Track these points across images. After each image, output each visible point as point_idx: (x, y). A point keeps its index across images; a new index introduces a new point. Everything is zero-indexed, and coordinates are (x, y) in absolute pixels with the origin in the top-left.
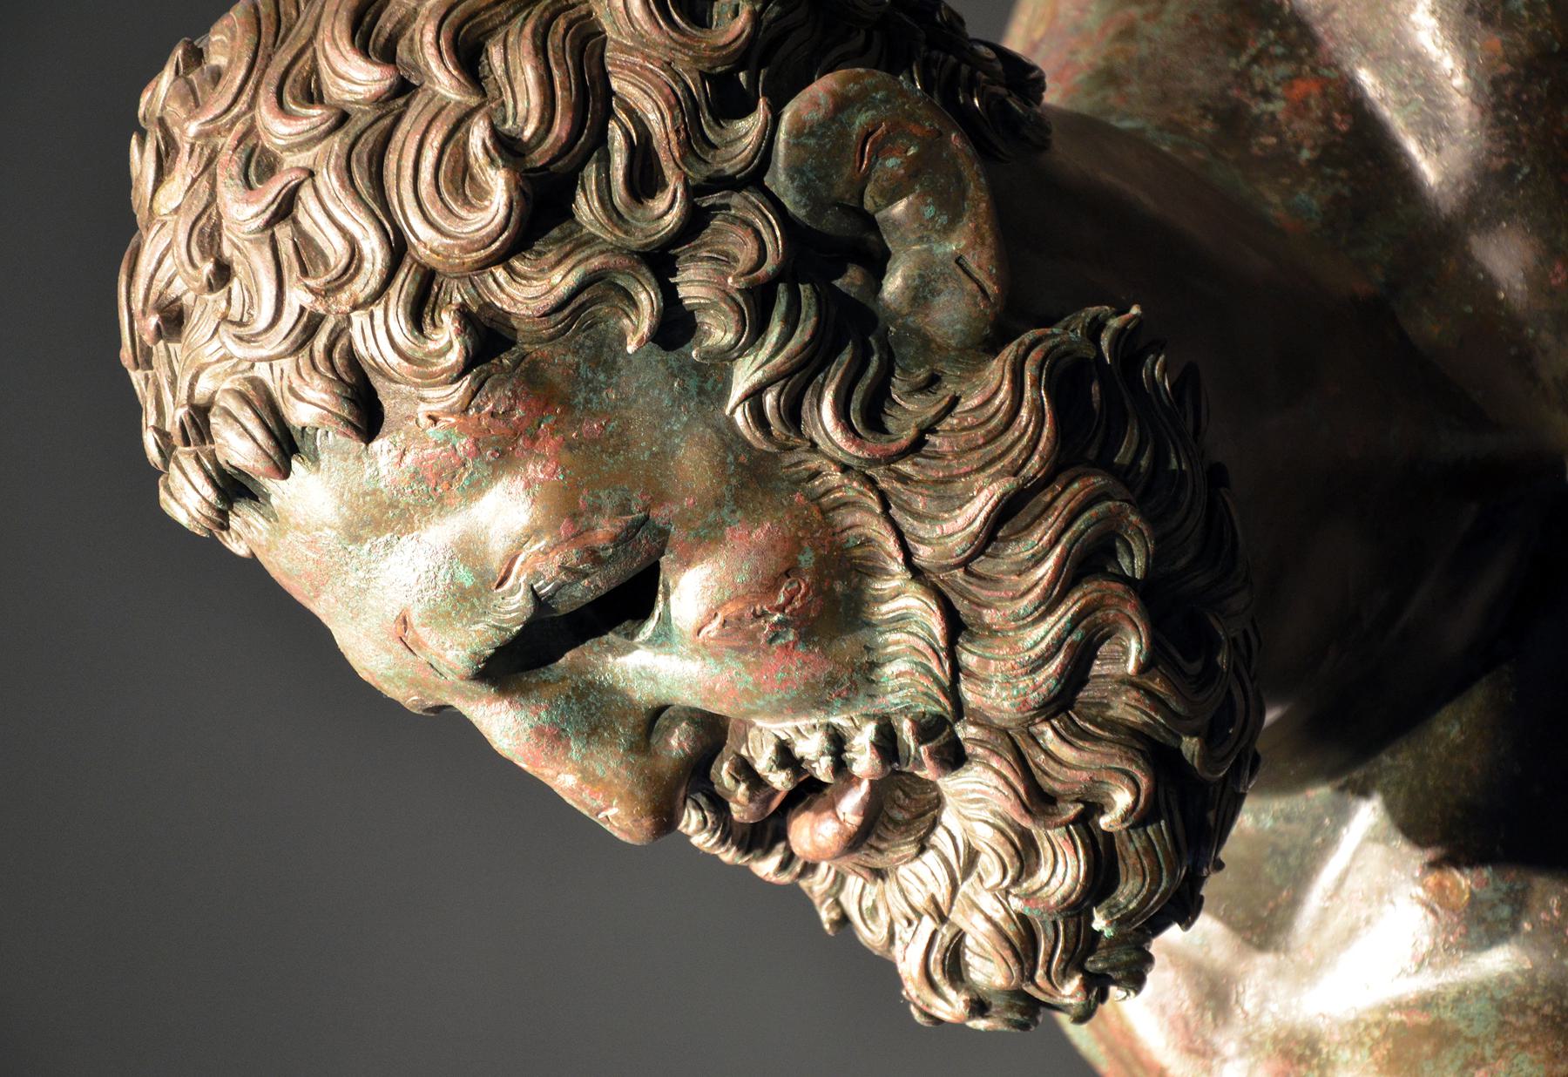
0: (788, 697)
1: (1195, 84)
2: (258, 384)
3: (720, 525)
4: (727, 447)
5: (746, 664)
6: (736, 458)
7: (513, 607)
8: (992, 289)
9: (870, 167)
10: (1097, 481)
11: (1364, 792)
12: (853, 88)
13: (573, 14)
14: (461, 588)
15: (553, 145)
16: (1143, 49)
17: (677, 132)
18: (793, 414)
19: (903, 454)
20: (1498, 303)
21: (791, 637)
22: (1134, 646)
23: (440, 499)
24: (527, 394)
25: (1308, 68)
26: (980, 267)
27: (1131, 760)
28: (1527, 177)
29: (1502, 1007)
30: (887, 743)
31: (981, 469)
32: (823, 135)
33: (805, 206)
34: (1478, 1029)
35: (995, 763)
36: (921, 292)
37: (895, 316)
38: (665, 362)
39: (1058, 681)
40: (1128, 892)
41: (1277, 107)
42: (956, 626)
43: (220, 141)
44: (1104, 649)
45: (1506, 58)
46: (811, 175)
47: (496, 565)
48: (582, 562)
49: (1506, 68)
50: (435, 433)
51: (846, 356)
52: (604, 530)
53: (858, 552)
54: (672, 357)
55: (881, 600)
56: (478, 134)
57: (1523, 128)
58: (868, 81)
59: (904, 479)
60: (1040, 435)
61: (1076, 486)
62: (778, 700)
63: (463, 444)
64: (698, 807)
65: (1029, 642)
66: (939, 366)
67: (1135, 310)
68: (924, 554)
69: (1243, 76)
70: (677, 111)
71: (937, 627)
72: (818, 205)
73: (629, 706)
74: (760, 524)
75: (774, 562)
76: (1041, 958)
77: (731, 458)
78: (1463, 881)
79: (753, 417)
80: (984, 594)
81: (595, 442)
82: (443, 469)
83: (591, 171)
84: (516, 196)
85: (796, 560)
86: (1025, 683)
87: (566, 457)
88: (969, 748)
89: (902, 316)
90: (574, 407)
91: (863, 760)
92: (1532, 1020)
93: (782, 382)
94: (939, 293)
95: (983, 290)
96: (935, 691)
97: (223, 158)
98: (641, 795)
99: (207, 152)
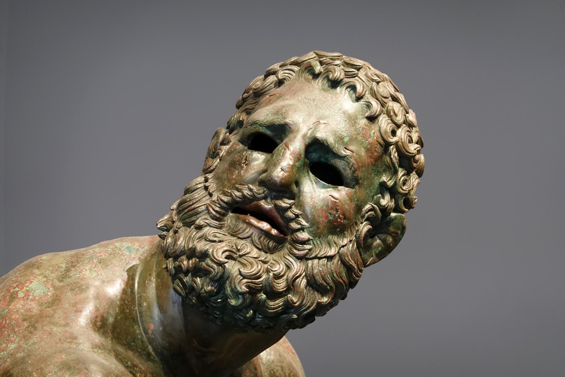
0: (315, 217)
5: (322, 207)
6: (363, 205)
21: (330, 218)
26: (371, 261)
42: (330, 258)
52: (359, 174)
62: (314, 215)
64: (264, 192)
75: (347, 214)
82: (365, 135)
91: (304, 235)
93: (375, 215)
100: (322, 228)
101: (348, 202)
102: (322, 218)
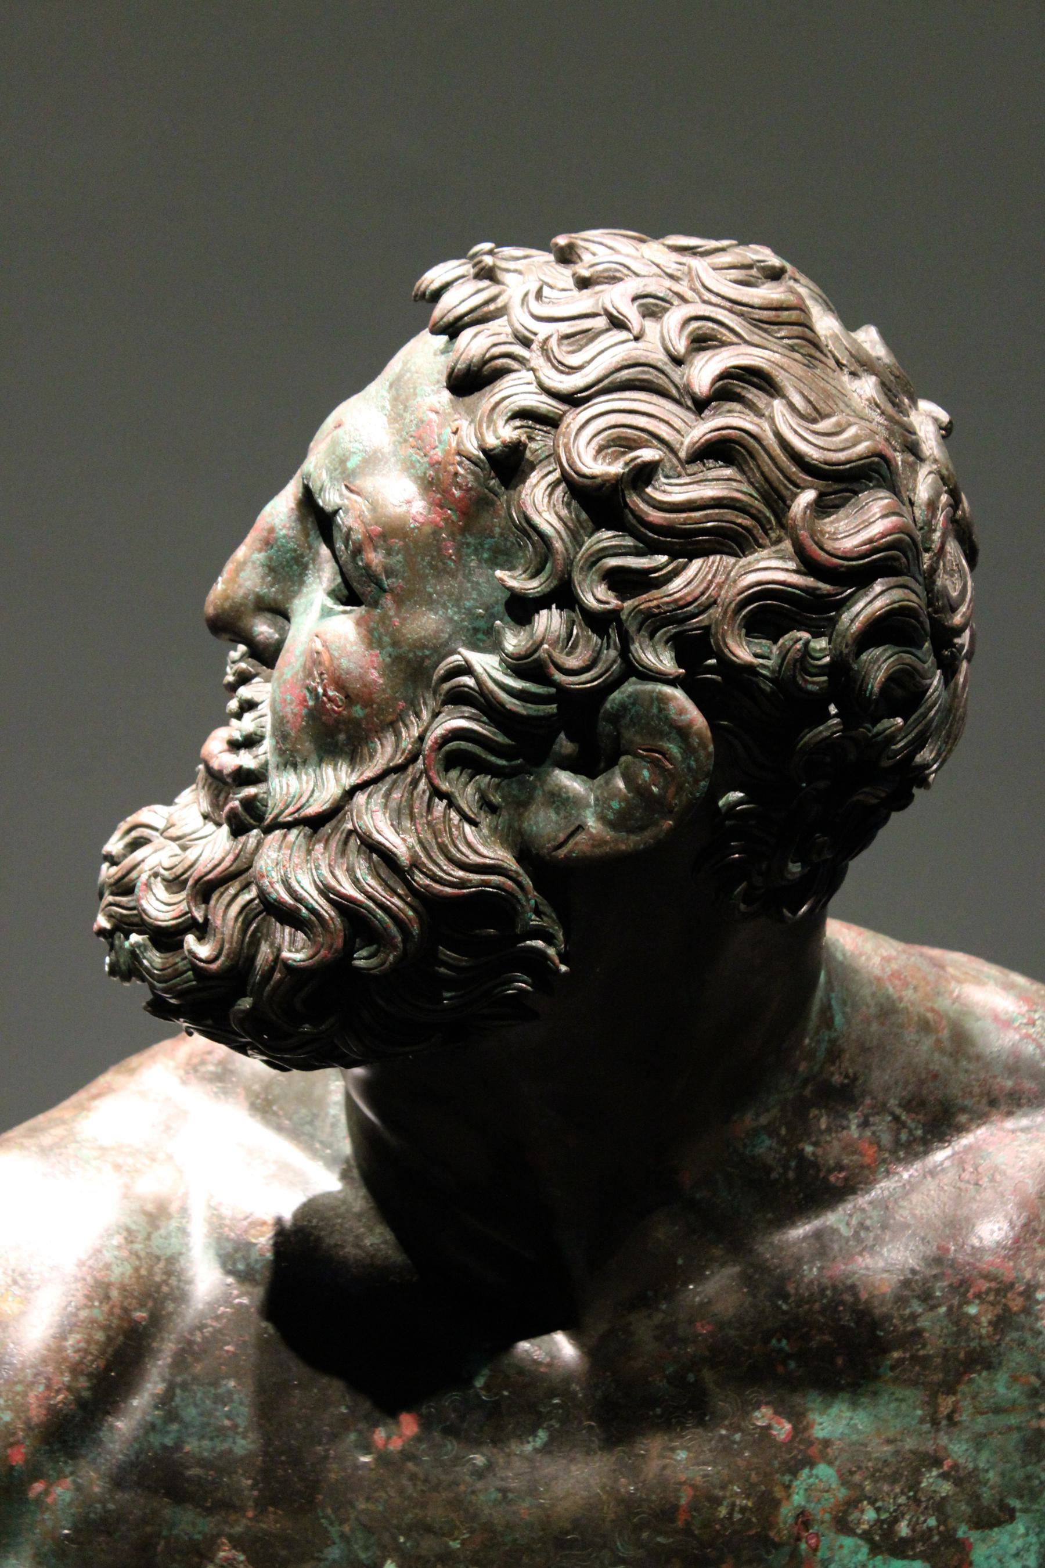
1: (877, 1073)
2: (501, 312)
3: (381, 646)
4: (435, 649)
6: (427, 657)
7: (330, 498)
8: (562, 853)
9: (642, 757)
10: (416, 930)
11: (344, 1176)
12: (695, 741)
13: (759, 532)
14: (347, 459)
15: (642, 510)
16: (910, 1035)
17: (658, 607)
18: (458, 698)
19: (430, 782)
20: (685, 1284)
22: (299, 956)
23: (406, 441)
24: (470, 499)
25: (887, 1155)
26: (576, 844)
27: (228, 956)
28: (779, 1308)
29: (172, 1260)
30: (245, 777)
31: (420, 842)
32: (660, 719)
33: (612, 708)
34: (156, 1241)
35: (231, 857)
36: (560, 800)
37: (542, 779)
38: (497, 603)
39: (275, 900)
40: (154, 959)
41: (854, 1131)
42: (315, 824)
43: (685, 283)
44: (300, 935)
45: (872, 1296)
46: (633, 711)
47: (358, 483)
48: (354, 543)
49: (864, 1296)
50: (448, 431)
51: (501, 739)
52: (375, 558)
53: (365, 751)
54: (500, 608)
55: (335, 769)
56: (648, 454)
57: (817, 1306)
58: (702, 753)
59: (415, 783)
60: (445, 885)
61: (411, 913)
63: (438, 454)
65: (300, 877)
66: (504, 813)
67: (563, 968)
68: (360, 798)
69: (882, 1108)
70: (673, 606)
71: (311, 811)
72: (616, 717)
73: (290, 595)
74: (381, 676)
76: (118, 899)
77: (427, 652)
78: (264, 1240)
79: (454, 667)
80: (333, 844)
81: (439, 550)
82: (423, 441)
83: (629, 542)
84: (599, 481)
85: (358, 703)
86: (275, 876)
87: (428, 529)
88: (242, 839)
89: (542, 786)
90: (464, 536)
92: (158, 1278)
94: (558, 813)
95: (561, 845)
96: (276, 811)
97: (668, 283)
98: (227, 605)
99: (679, 274)
100: (293, 734)
101: (355, 648)
102: (291, 704)
